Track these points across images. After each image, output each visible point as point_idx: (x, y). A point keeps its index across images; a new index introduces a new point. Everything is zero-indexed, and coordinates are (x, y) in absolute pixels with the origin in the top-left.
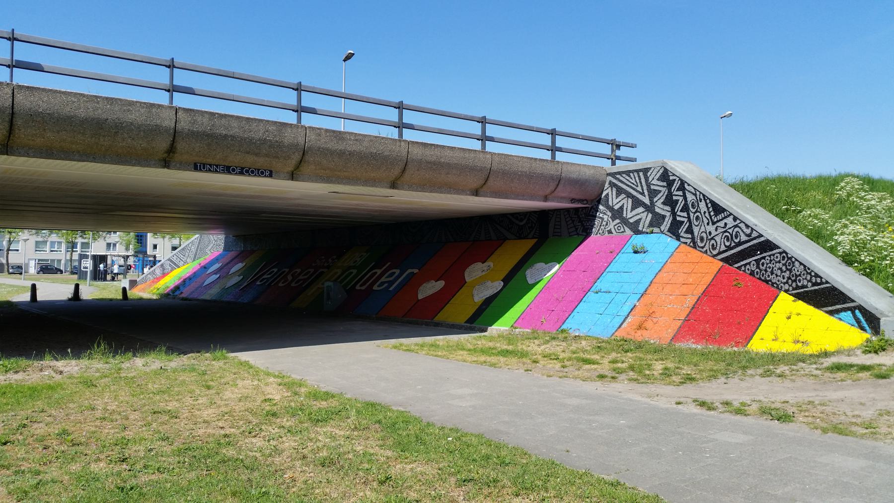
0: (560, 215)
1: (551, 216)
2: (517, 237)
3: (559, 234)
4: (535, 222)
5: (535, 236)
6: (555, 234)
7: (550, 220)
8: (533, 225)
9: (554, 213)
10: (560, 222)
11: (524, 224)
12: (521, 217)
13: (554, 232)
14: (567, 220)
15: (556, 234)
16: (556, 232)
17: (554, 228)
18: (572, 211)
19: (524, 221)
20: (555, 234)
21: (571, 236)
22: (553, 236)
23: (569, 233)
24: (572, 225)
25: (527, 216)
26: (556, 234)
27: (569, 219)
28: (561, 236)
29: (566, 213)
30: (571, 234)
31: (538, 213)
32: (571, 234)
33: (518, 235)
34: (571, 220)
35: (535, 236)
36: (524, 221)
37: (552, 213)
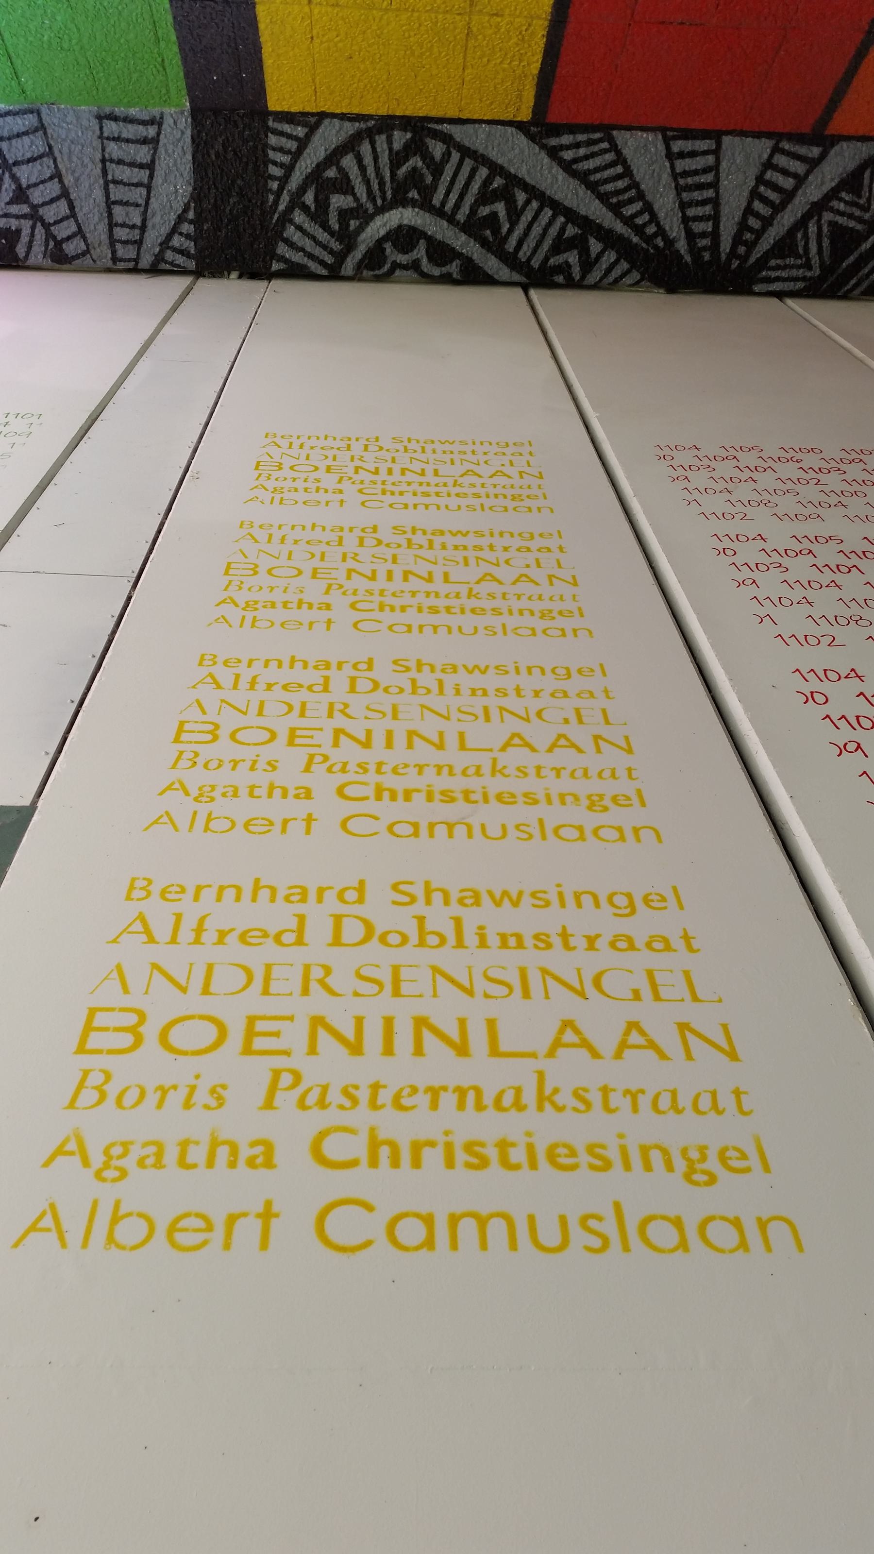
0: (113, 242)
1: (176, 241)
2: (447, 139)
3: (111, 128)
4: (299, 217)
5: (300, 131)
6: (152, 131)
7: (181, 219)
8: (309, 198)
9: (159, 258)
10: (109, 204)
11: (381, 210)
12: (402, 259)
13: (153, 142)
14: (62, 207)
15: (143, 131)
16: (144, 141)
17: (150, 167)
18: (37, 255)
19: (379, 226)
20: (152, 131)
21: (152, 122)
22: (157, 122)
23: (41, 127)
24: (25, 174)
25: (358, 254)
26: (143, 131)
27: (50, 214)
28: (100, 118)
29: (70, 248)
30: (30, 121)
31: (275, 266)
32: (30, 121)
33: (437, 149)
34: (35, 208)
35: (300, 131)
36: (379, 226)
37: (169, 255)
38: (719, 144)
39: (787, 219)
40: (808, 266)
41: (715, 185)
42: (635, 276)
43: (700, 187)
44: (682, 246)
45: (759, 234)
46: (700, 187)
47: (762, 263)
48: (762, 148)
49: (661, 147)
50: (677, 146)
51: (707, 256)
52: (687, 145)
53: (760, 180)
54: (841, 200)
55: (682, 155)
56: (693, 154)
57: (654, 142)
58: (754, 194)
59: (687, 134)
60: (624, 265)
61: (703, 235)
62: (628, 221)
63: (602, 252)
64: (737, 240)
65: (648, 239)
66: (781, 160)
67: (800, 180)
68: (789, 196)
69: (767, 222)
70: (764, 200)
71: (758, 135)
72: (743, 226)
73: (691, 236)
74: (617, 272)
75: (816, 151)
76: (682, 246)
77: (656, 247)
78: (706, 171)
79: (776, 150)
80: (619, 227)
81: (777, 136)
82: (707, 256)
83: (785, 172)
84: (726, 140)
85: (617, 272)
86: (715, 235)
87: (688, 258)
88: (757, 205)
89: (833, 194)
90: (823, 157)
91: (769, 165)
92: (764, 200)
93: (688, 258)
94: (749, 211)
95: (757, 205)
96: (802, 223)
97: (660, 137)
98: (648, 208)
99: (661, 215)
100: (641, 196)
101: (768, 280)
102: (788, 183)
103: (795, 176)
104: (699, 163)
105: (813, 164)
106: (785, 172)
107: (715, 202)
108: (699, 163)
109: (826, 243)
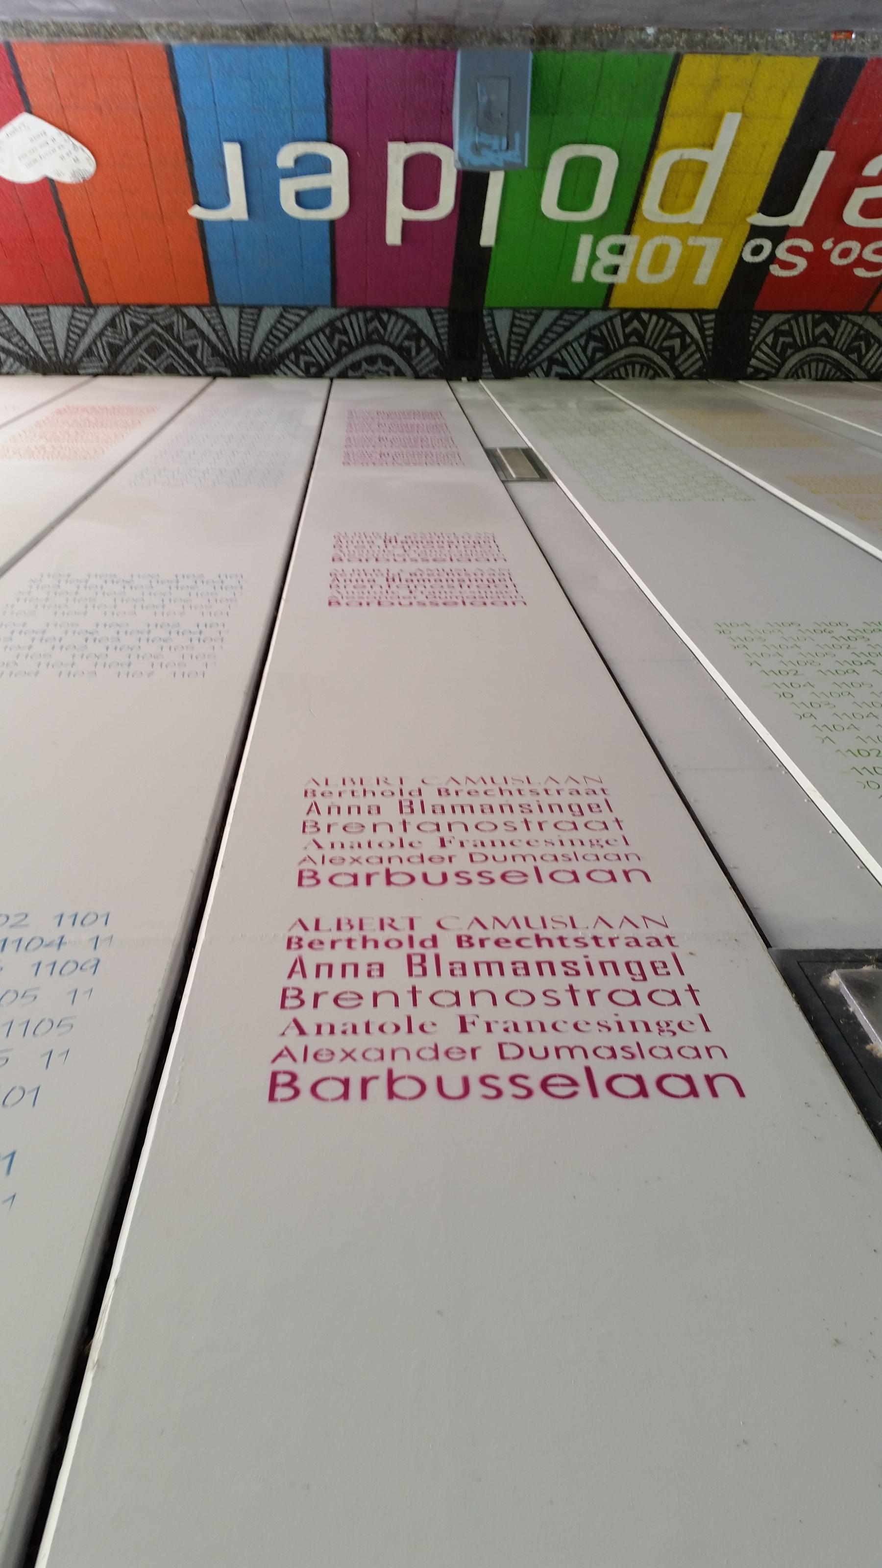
38: (48, 309)
39: (87, 341)
40: (102, 361)
41: (51, 327)
42: (24, 368)
43: (44, 328)
44: (42, 354)
45: (75, 348)
46: (44, 328)
47: (80, 360)
48: (67, 311)
49: (23, 313)
50: (30, 311)
51: (54, 358)
52: (34, 311)
53: (70, 324)
54: (107, 330)
55: (33, 315)
56: (38, 315)
57: (20, 311)
58: (69, 330)
59: (33, 306)
60: (18, 364)
61: (50, 349)
62: (16, 345)
63: (7, 359)
64: (67, 350)
65: (26, 353)
66: (77, 315)
67: (88, 324)
68: (84, 331)
69: (77, 343)
70: (74, 333)
71: (64, 304)
72: (67, 344)
73: (45, 350)
74: (15, 367)
75: (92, 311)
76: (42, 354)
77: (31, 356)
78: (45, 321)
79: (74, 310)
80: (12, 347)
81: (73, 305)
82: (54, 358)
83: (80, 320)
84: (51, 308)
85: (15, 367)
86: (56, 349)
87: (45, 359)
88: (72, 335)
89: (105, 328)
90: (96, 313)
91: (73, 317)
92: (74, 333)
93: (45, 359)
94: (68, 337)
95: (72, 335)
96: (94, 342)
97: (21, 308)
98: (23, 339)
99: (30, 343)
100: (18, 333)
101: (85, 368)
102: (83, 325)
103: (86, 322)
104: (41, 318)
105: (92, 317)
106: (80, 320)
107: (53, 335)
108: (41, 318)
109: (107, 351)
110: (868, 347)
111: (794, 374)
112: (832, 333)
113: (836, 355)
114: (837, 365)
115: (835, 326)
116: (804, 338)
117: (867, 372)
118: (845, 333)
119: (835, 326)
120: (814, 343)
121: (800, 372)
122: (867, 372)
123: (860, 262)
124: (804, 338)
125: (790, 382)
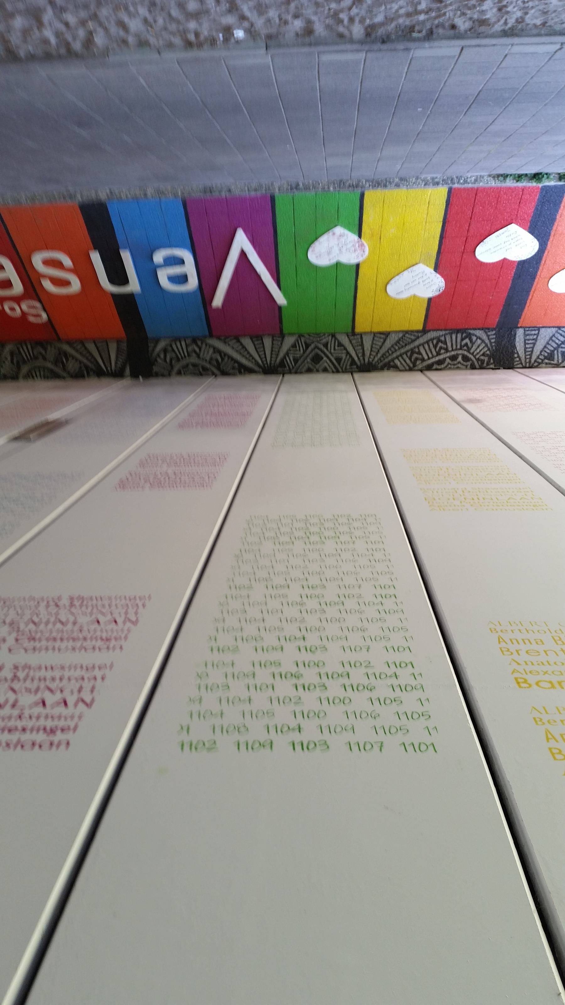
110: (67, 360)
111: (30, 376)
112: (43, 352)
113: (49, 365)
114: (52, 371)
115: (45, 350)
116: (28, 355)
117: (69, 373)
118: (51, 352)
119: (45, 350)
120: (36, 358)
121: (30, 374)
122: (69, 373)
123: (23, 313)
124: (28, 355)
125: (30, 382)
